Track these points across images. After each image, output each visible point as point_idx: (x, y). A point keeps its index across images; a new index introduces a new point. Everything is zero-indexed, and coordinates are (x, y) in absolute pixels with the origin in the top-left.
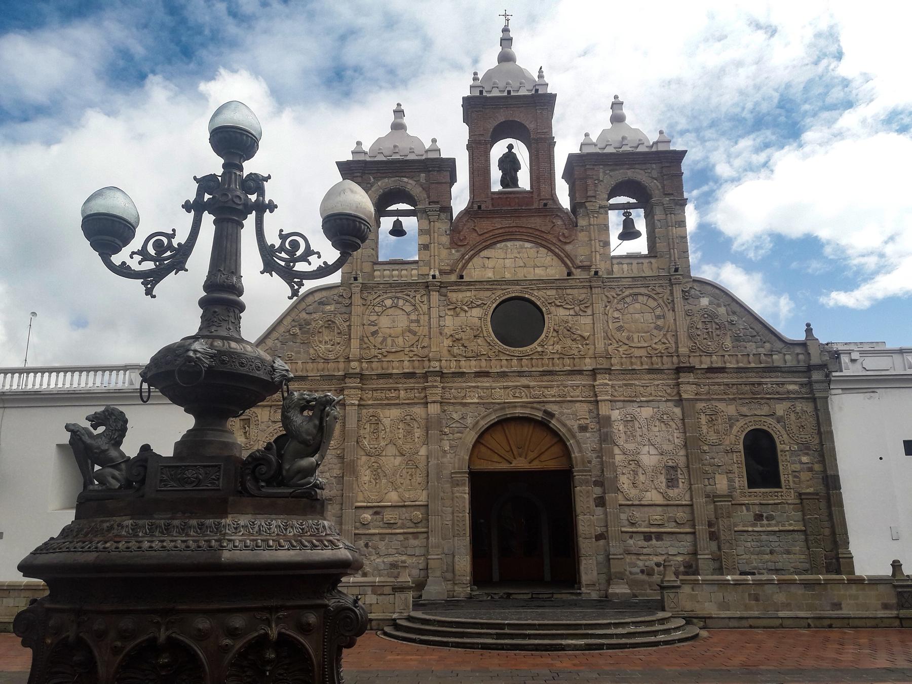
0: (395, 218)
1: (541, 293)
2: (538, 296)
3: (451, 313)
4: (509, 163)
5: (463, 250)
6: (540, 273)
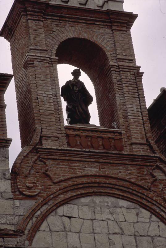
5: (30, 204)
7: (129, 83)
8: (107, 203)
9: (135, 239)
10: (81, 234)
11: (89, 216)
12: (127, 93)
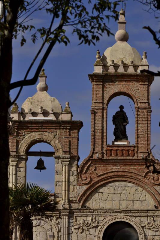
0: (38, 158)
1: (137, 219)
2: (134, 222)
3: (76, 231)
4: (120, 119)
6: (137, 206)
7: (143, 117)
8: (122, 185)
9: (133, 202)
10: (107, 201)
11: (112, 192)
12: (142, 123)
